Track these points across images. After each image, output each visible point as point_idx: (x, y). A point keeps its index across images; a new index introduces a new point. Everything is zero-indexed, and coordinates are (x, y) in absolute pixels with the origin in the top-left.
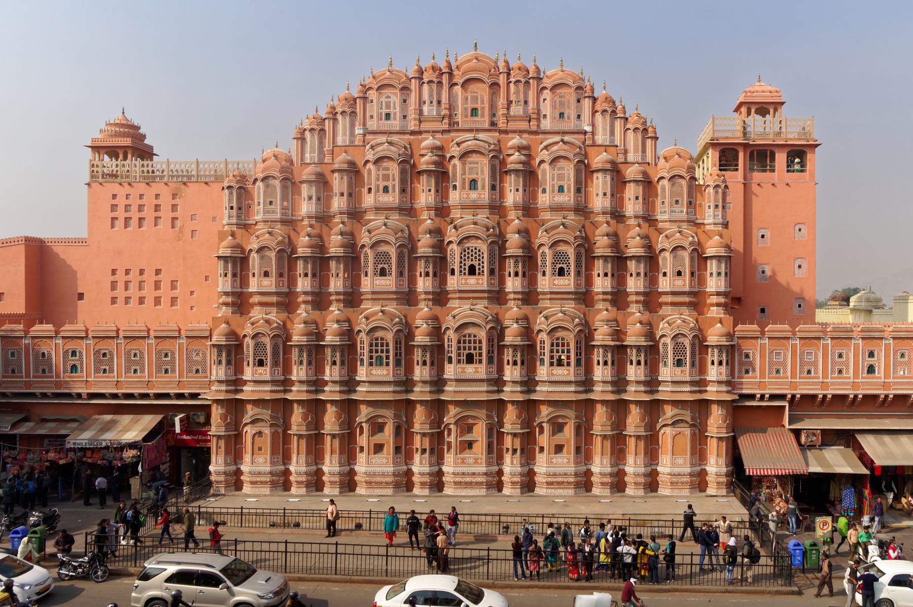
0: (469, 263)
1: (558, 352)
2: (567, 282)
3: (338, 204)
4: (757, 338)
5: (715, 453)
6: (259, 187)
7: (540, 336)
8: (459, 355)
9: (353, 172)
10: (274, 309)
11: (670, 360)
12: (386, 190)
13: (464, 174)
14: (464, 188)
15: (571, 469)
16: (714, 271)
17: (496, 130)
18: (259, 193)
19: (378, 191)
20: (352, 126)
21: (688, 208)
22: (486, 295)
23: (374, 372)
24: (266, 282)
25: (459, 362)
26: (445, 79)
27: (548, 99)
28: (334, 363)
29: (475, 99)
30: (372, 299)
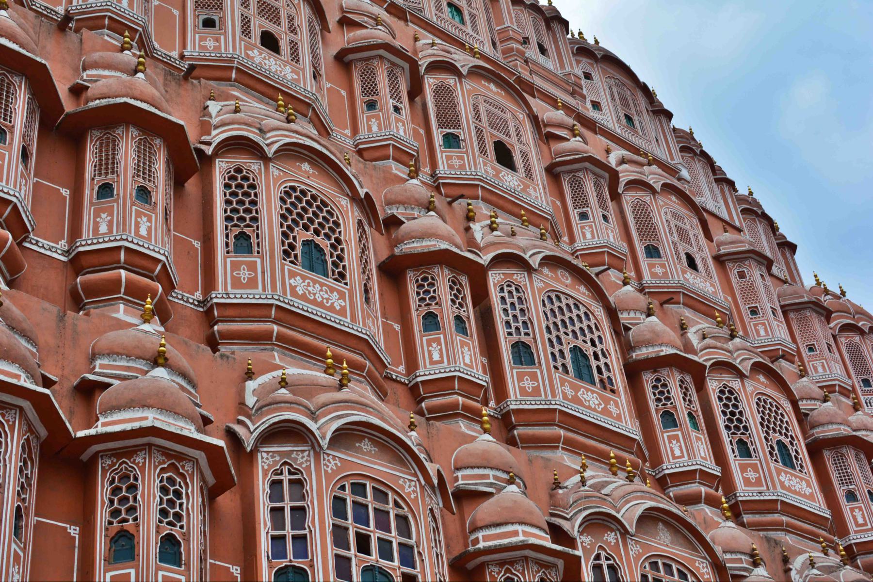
12: (270, 42)
13: (478, 117)
27: (596, 75)
30: (281, 338)
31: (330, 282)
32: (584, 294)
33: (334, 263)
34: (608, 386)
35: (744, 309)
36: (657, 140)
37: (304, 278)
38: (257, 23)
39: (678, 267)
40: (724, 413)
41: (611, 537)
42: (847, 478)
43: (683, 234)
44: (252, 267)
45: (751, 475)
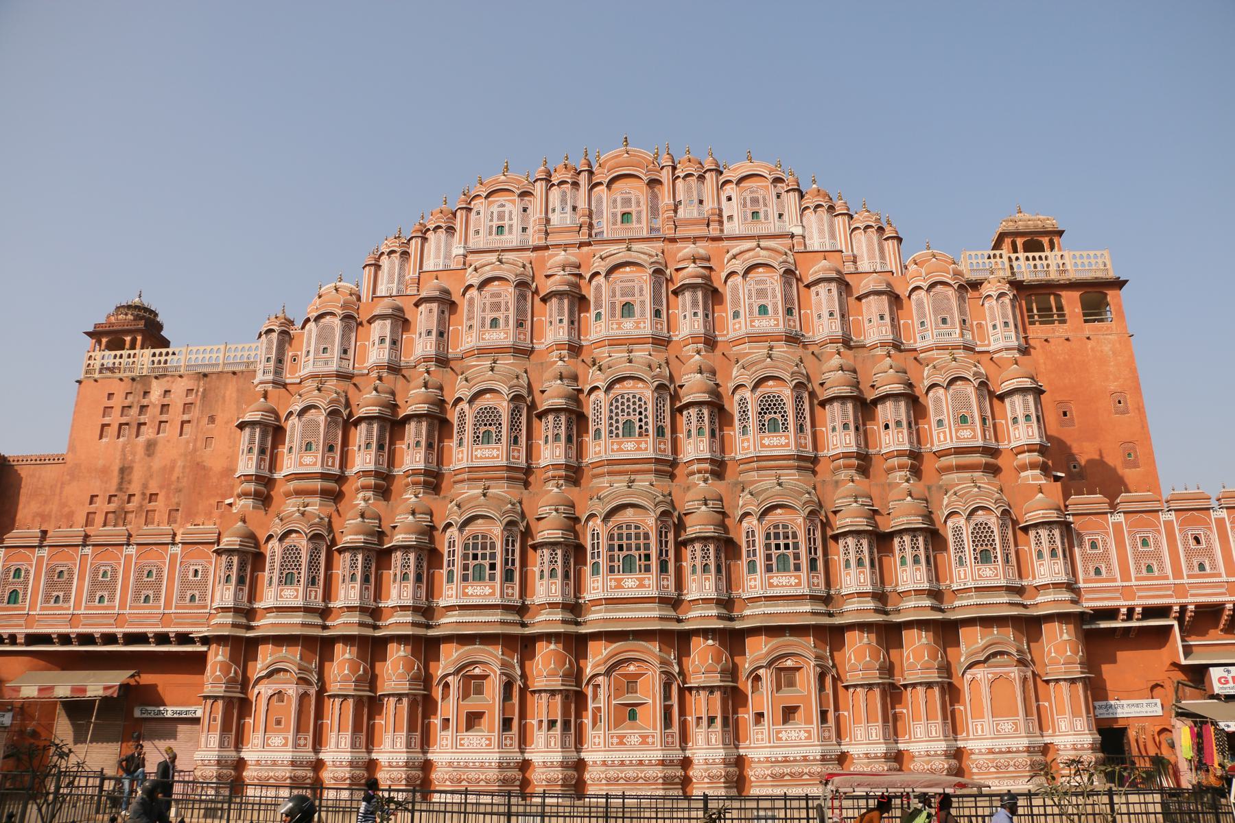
1: (778, 547)
2: (783, 441)
3: (421, 345)
4: (1106, 513)
5: (1068, 709)
6: (310, 331)
8: (611, 559)
9: (447, 303)
10: (317, 500)
11: (969, 554)
12: (494, 323)
13: (614, 295)
14: (613, 315)
15: (815, 752)
16: (1020, 413)
17: (657, 239)
18: (309, 339)
19: (483, 325)
20: (448, 246)
21: (962, 329)
22: (653, 467)
23: (470, 590)
24: (308, 459)
25: (612, 570)
26: (583, 179)
28: (405, 577)
29: (627, 201)
31: (494, 445)
36: (780, 215)
42: (833, 420)
43: (761, 293)
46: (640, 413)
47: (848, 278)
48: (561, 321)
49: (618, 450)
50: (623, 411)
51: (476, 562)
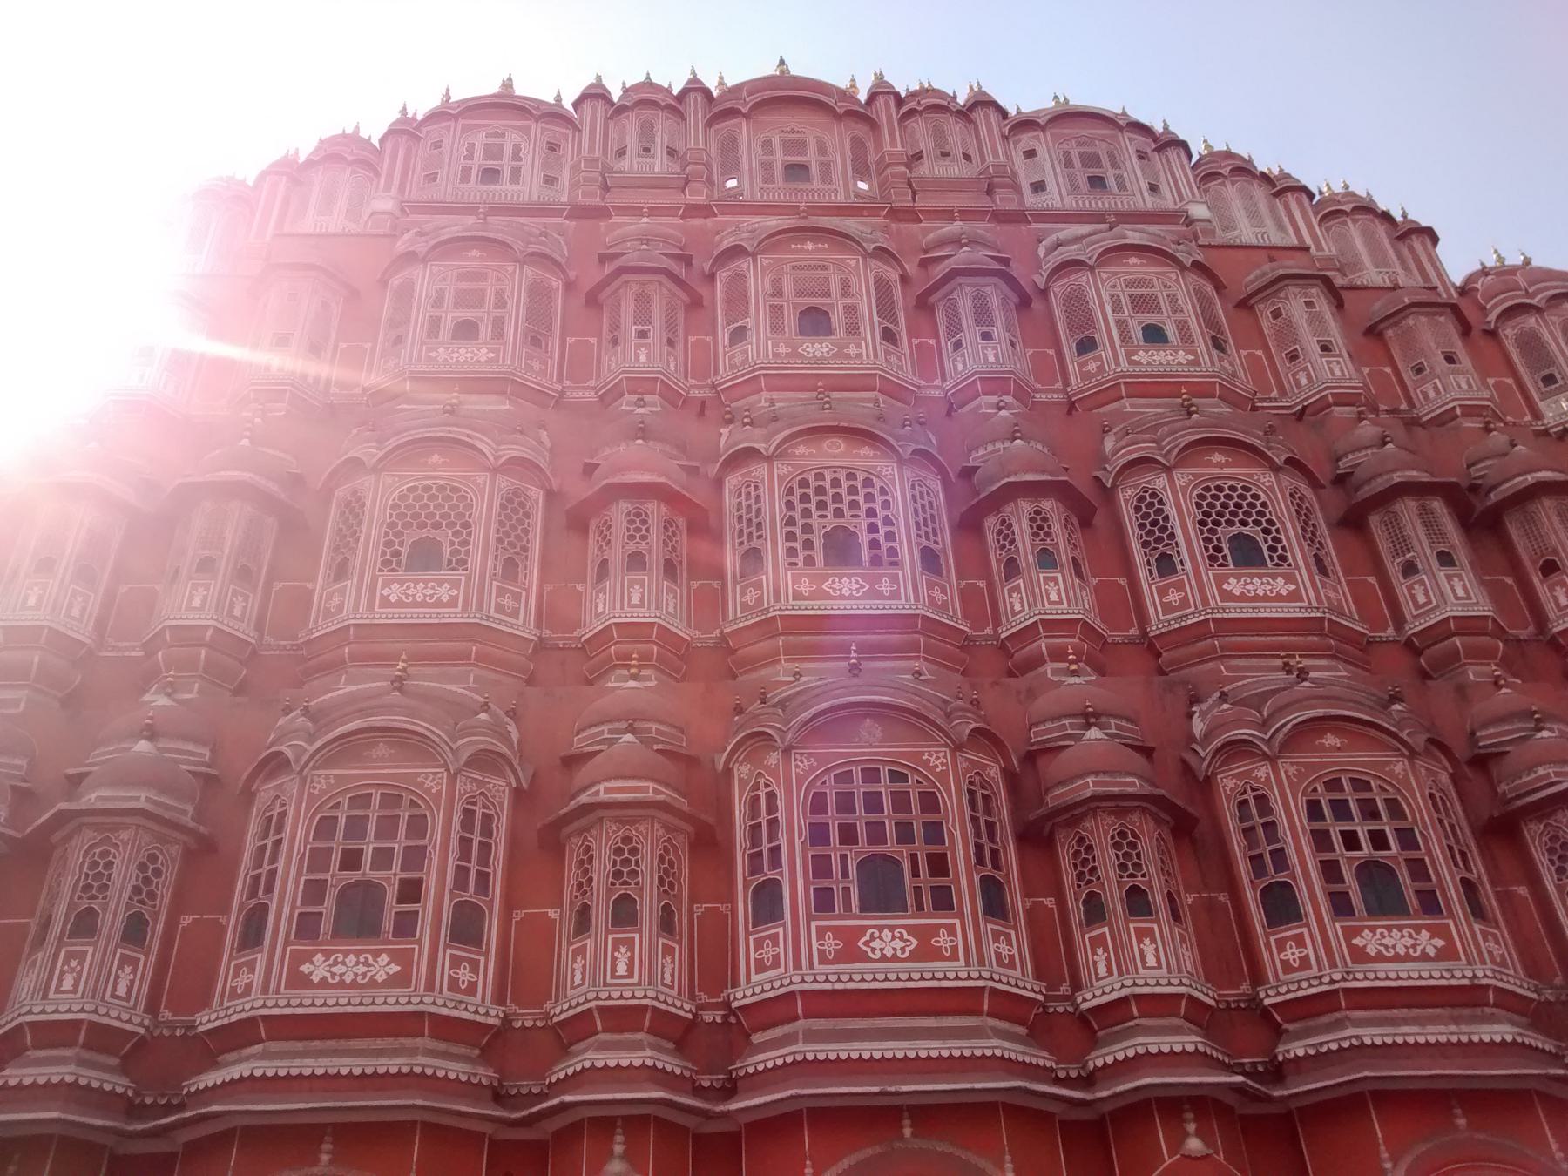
0: (821, 524)
1: (1351, 841)
7: (1227, 783)
8: (821, 866)
12: (466, 330)
13: (778, 292)
23: (317, 969)
25: (823, 901)
27: (1042, 151)
30: (353, 657)
31: (444, 574)
32: (866, 457)
33: (455, 552)
34: (885, 558)
35: (1280, 359)
36: (1154, 188)
37: (401, 583)
38: (450, 316)
39: (1121, 352)
40: (1141, 526)
41: (773, 759)
42: (1402, 544)
43: (1143, 303)
44: (342, 592)
45: (1173, 597)
46: (871, 513)
47: (1344, 294)
48: (643, 334)
49: (813, 596)
50: (822, 505)
51: (354, 876)
